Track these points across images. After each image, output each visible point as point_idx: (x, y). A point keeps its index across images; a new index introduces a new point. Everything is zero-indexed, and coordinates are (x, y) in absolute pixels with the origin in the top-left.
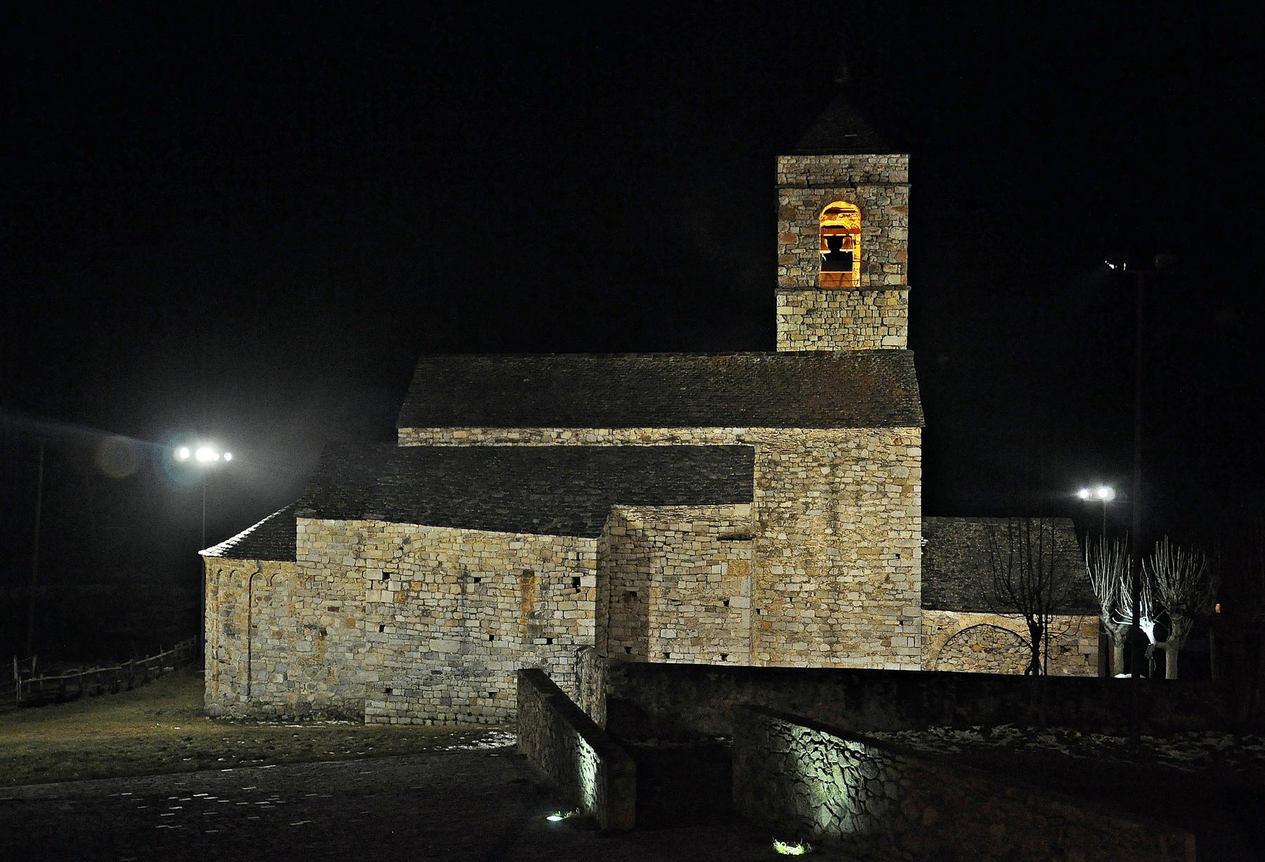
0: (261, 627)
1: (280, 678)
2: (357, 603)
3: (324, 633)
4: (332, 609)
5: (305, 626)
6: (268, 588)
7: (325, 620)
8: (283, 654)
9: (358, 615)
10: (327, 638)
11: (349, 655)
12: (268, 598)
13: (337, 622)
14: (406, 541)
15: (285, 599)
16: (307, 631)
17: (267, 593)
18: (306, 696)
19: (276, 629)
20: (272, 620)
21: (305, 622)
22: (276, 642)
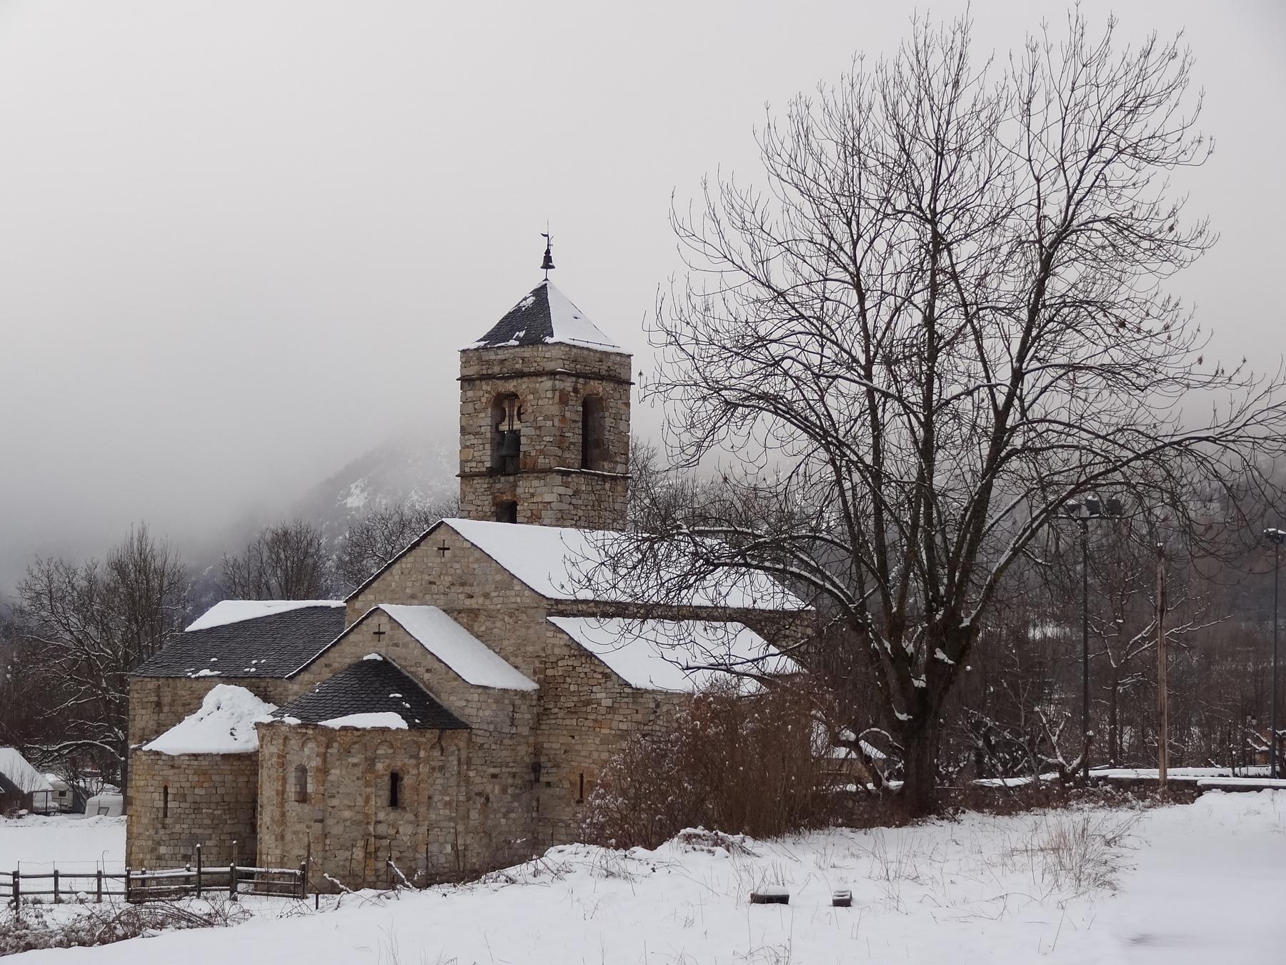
0: (436, 798)
1: (449, 849)
2: (509, 770)
3: (487, 799)
4: (494, 776)
5: (476, 794)
6: (443, 758)
7: (489, 788)
8: (452, 824)
9: (510, 781)
10: (490, 805)
11: (503, 821)
12: (442, 768)
13: (497, 788)
14: (658, 706)
15: (455, 768)
16: (478, 798)
17: (441, 764)
18: (474, 864)
19: (447, 799)
20: (445, 791)
21: (476, 790)
22: (447, 812)
